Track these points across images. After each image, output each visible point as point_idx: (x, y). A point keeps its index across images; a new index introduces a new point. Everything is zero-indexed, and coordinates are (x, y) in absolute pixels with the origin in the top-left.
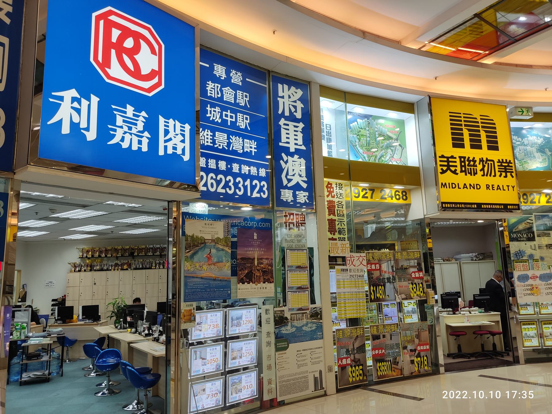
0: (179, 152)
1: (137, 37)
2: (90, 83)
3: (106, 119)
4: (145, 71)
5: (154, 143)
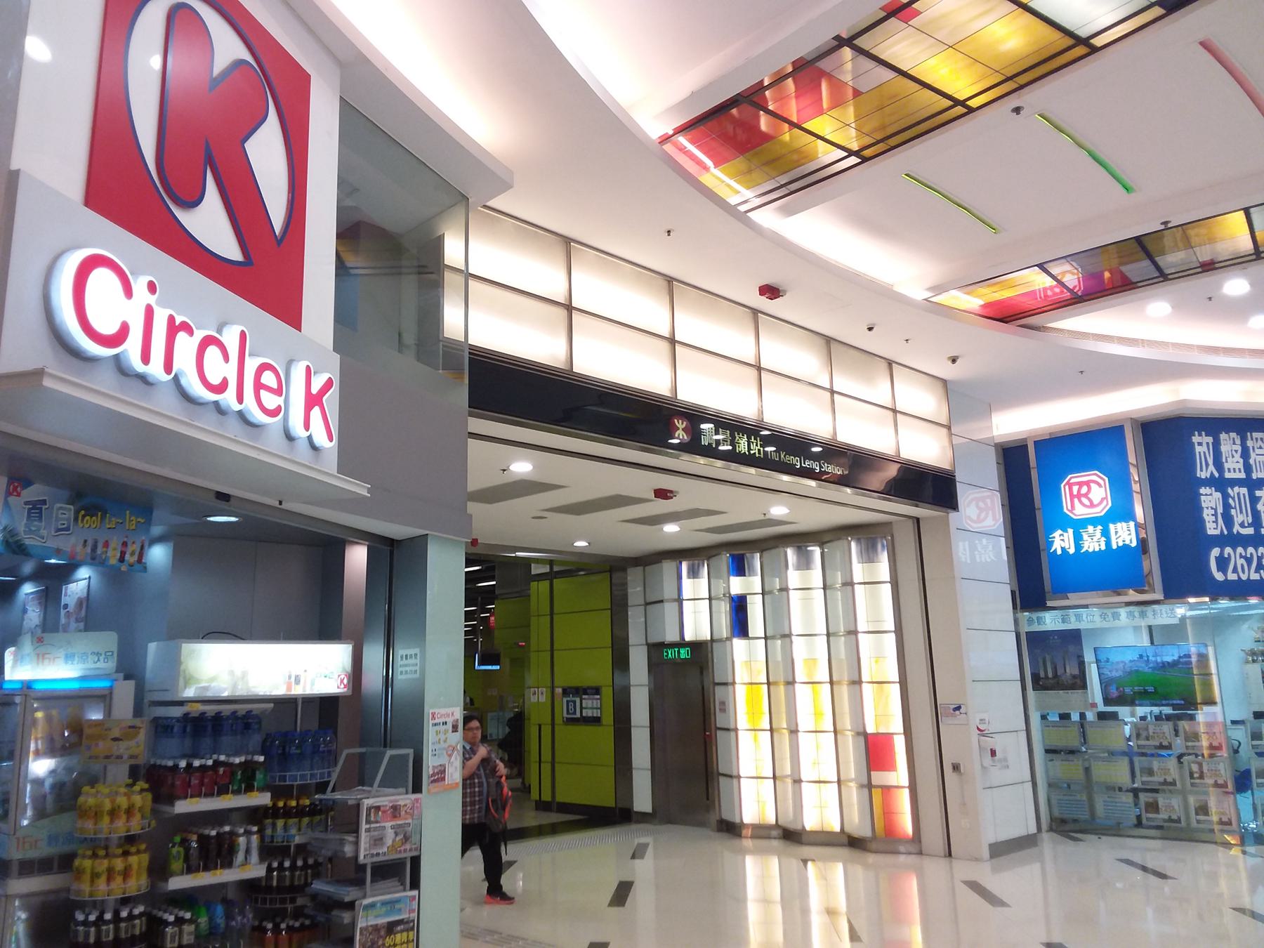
0: (1127, 542)
1: (1088, 483)
2: (1066, 523)
3: (1078, 539)
4: (1095, 502)
5: (1108, 543)
